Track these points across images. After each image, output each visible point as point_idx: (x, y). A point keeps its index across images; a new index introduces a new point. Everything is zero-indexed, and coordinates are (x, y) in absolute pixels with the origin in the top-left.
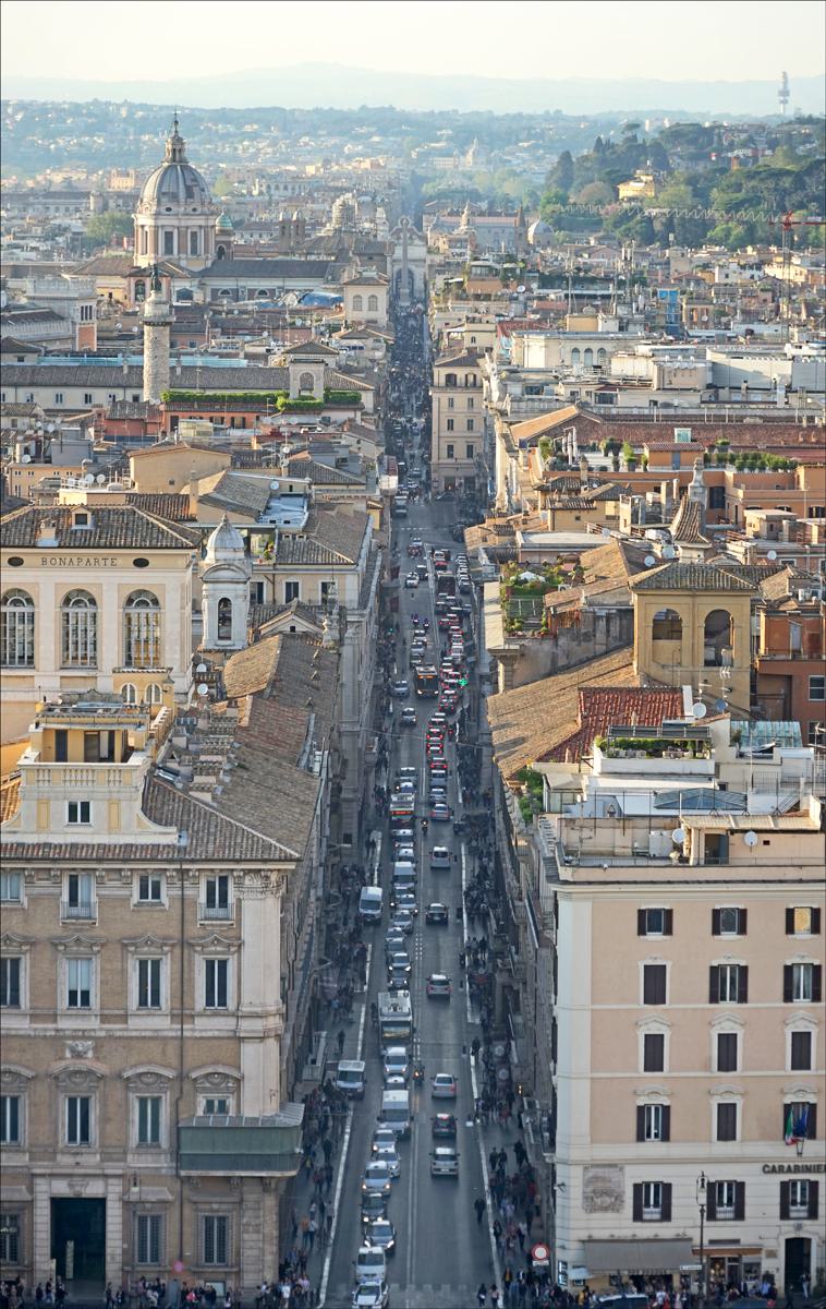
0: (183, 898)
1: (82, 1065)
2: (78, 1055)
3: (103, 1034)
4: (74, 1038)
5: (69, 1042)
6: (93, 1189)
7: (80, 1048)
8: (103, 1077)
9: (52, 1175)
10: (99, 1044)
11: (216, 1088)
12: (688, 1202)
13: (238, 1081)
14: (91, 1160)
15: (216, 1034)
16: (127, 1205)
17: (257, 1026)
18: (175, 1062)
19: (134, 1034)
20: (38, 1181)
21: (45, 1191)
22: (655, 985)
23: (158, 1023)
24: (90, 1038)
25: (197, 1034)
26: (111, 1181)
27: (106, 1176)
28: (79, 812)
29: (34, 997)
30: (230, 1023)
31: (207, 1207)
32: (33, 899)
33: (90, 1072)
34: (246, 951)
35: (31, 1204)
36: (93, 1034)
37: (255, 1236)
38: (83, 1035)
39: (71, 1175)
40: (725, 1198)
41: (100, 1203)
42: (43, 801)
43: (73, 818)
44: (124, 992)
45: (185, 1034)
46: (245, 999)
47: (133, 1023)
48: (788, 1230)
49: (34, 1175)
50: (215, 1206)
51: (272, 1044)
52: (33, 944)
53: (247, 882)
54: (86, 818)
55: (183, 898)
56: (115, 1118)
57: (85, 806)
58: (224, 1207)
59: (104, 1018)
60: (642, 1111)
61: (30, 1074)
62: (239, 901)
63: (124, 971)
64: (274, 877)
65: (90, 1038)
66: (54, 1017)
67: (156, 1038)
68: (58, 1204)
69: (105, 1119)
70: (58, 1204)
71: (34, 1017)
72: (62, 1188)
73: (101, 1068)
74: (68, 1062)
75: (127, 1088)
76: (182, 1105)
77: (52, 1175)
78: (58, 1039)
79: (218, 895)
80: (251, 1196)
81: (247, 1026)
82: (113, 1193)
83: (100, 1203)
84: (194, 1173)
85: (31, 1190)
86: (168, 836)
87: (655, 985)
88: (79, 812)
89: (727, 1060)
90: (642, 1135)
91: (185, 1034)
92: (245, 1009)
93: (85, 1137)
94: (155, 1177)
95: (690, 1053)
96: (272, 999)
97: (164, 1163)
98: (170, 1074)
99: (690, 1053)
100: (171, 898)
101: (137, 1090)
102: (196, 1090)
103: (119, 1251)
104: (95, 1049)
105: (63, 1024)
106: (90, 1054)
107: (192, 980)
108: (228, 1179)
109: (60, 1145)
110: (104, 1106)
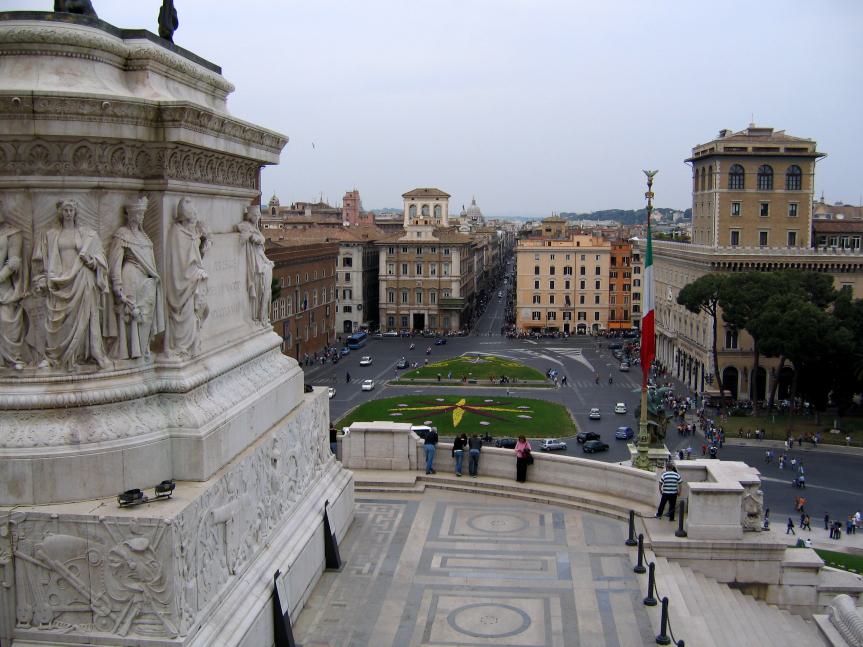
6: (422, 312)
10: (423, 282)
12: (544, 315)
16: (429, 315)
21: (412, 313)
22: (537, 270)
23: (434, 278)
28: (419, 234)
40: (551, 315)
41: (423, 315)
42: (412, 232)
48: (565, 322)
51: (458, 283)
60: (534, 297)
68: (415, 315)
70: (415, 315)
72: (416, 312)
79: (447, 252)
83: (423, 315)
87: (537, 270)
88: (419, 234)
89: (552, 286)
90: (534, 301)
95: (544, 286)
96: (458, 274)
97: (436, 307)
99: (544, 286)
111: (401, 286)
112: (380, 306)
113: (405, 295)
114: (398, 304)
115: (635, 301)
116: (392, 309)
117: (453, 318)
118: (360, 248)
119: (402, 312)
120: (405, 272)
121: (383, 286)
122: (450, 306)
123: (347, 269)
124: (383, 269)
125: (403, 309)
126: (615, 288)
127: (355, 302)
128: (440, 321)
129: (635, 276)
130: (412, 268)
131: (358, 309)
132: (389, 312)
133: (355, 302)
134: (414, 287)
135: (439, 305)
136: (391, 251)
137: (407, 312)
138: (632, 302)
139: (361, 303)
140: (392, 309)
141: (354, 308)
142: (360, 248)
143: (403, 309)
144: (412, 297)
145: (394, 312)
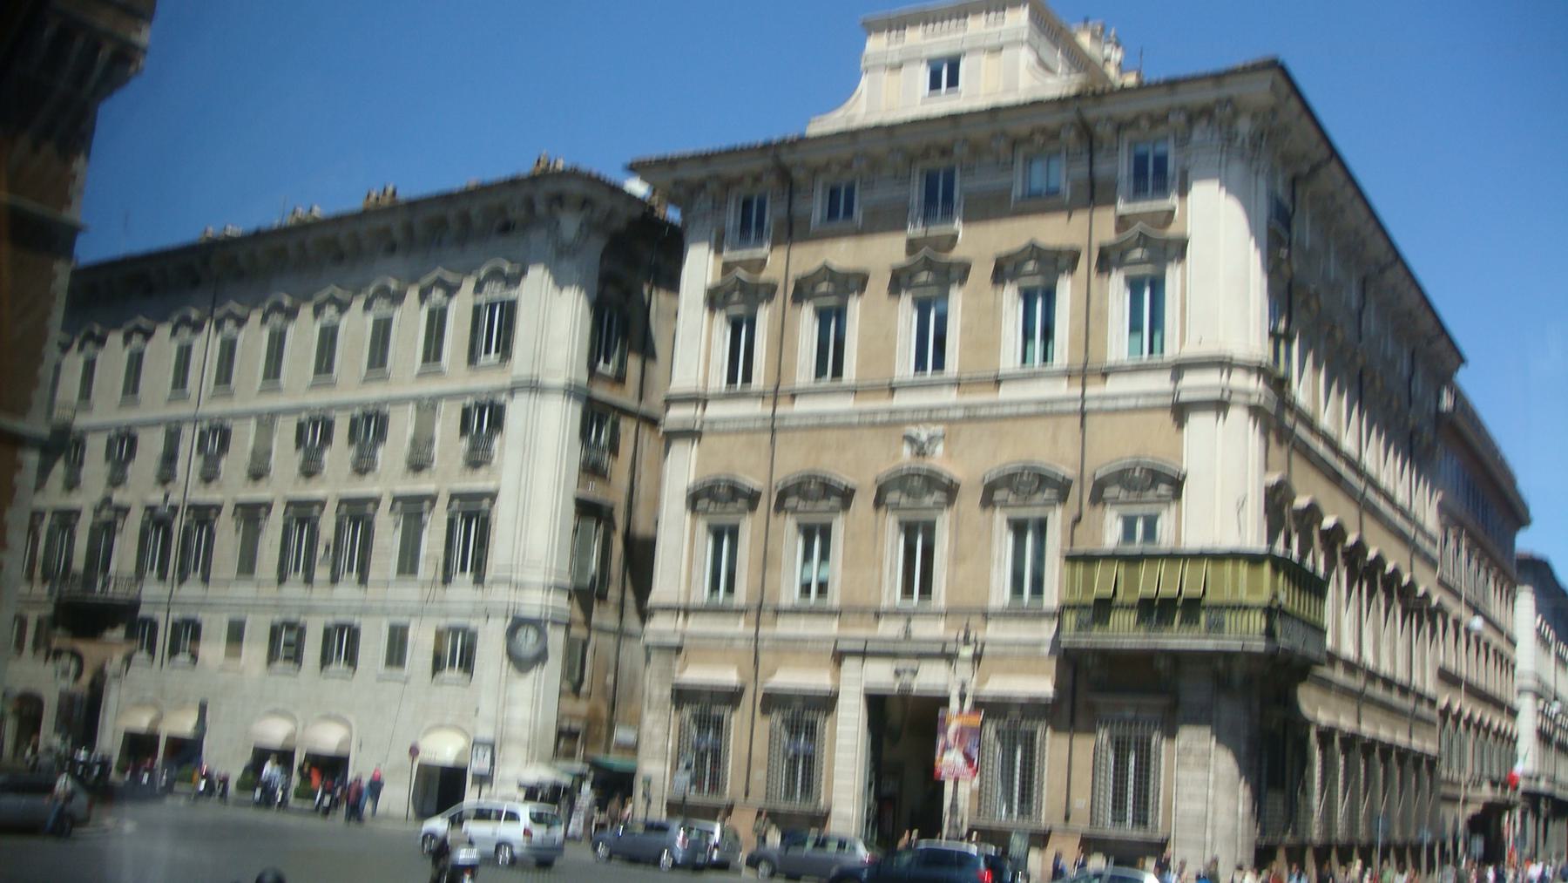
4: (916, 423)
6: (931, 678)
18: (1073, 454)
19: (1007, 410)
25: (1109, 404)
29: (863, 364)
36: (943, 414)
37: (1199, 775)
38: (930, 416)
45: (1088, 405)
47: (1007, 393)
56: (978, 556)
63: (995, 312)
64: (1244, 126)
67: (1045, 412)
69: (957, 558)
72: (881, 675)
77: (864, 655)
78: (893, 422)
81: (1197, 384)
85: (836, 677)
92: (1191, 350)
93: (926, 589)
105: (902, 400)
107: (1103, 315)
113: (816, 535)
122: (1155, 610)
125: (793, 648)
127: (499, 595)
128: (1070, 767)
130: (882, 327)
132: (696, 674)
133: (499, 595)
139: (535, 602)
140: (717, 648)
142: (570, 225)
143: (793, 648)
144: (868, 553)
145: (728, 676)
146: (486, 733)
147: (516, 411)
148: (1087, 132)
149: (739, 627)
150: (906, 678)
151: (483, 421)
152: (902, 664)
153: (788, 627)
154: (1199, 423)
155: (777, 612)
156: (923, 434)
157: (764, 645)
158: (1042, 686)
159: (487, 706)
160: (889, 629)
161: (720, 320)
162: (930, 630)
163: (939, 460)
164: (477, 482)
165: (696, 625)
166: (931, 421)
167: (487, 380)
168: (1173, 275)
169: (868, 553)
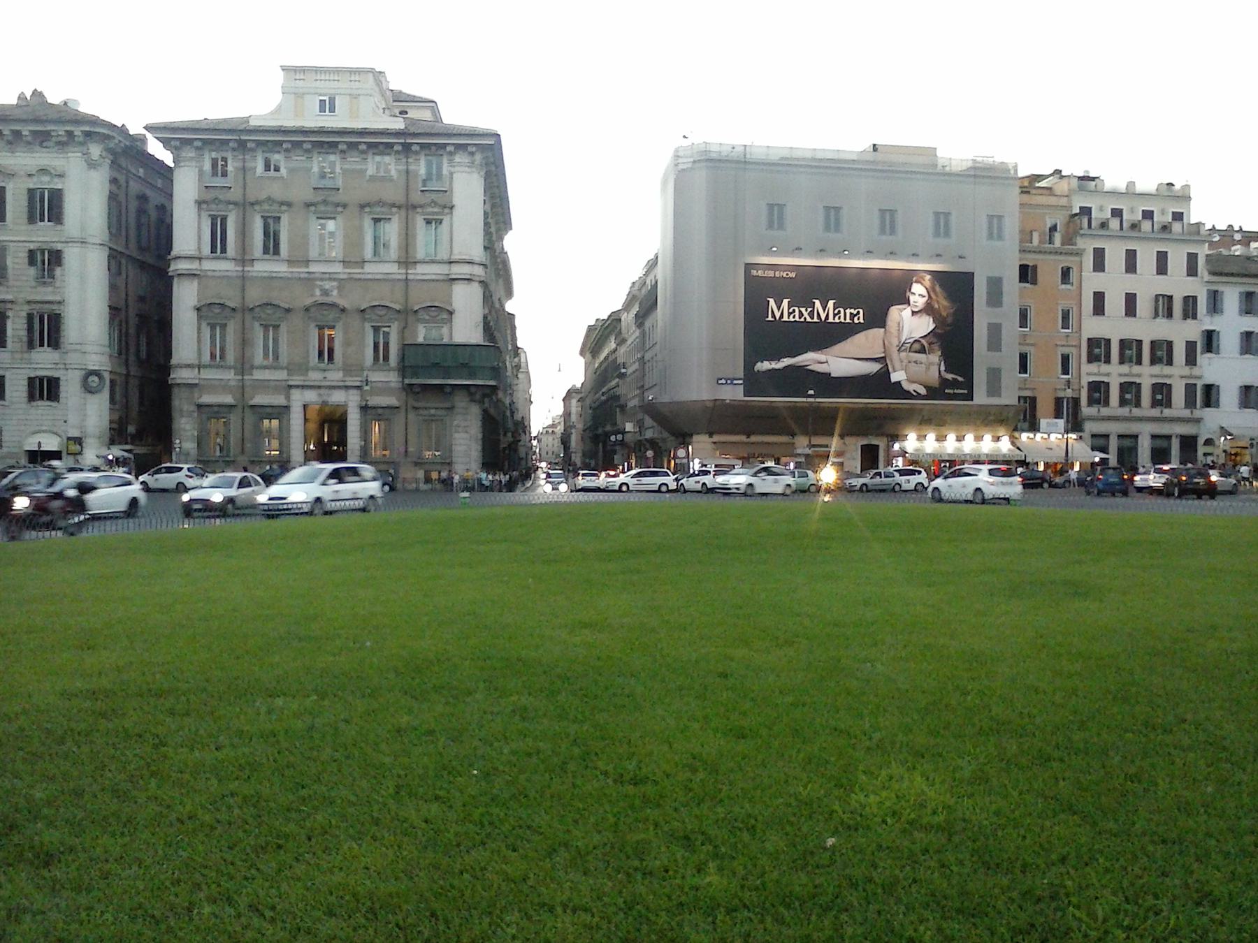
0: (407, 172)
1: (329, 300)
2: (326, 293)
3: (345, 276)
4: (322, 280)
5: (318, 283)
6: (337, 397)
7: (327, 287)
8: (343, 310)
9: (303, 387)
11: (434, 320)
13: (451, 313)
14: (335, 376)
15: (434, 277)
16: (364, 409)
17: (464, 270)
19: (370, 277)
20: (293, 391)
24: (335, 280)
26: (352, 392)
27: (347, 387)
28: (328, 106)
30: (442, 269)
31: (425, 412)
32: (291, 171)
33: (333, 305)
34: (455, 212)
35: (287, 408)
37: (465, 435)
38: (331, 277)
39: (319, 387)
43: (322, 110)
44: (360, 244)
46: (456, 251)
47: (369, 268)
49: (291, 387)
50: (433, 411)
52: (289, 205)
53: (457, 158)
54: (332, 110)
55: (407, 172)
57: (332, 101)
58: (439, 412)
59: (345, 263)
61: (287, 306)
62: (451, 174)
65: (335, 280)
66: (307, 262)
67: (386, 280)
71: (290, 262)
73: (342, 302)
74: (318, 296)
75: (365, 320)
76: (403, 325)
77: (303, 387)
78: (309, 280)
80: (461, 401)
81: (458, 270)
82: (351, 402)
84: (414, 381)
85: (288, 398)
86: (398, 124)
91: (410, 277)
92: (455, 257)
94: (384, 390)
97: (393, 378)
98: (397, 307)
100: (399, 171)
101: (370, 320)
102: (418, 320)
103: (358, 447)
104: (338, 288)
106: (335, 293)
108: (441, 387)
109: (311, 364)
110: (346, 332)
111: (255, 296)
112: (180, 376)
114: (243, 366)
115: (1093, 368)
116: (224, 387)
117: (458, 421)
118: (95, 150)
119: (259, 400)
120: (272, 245)
121: (185, 298)
123: (43, 234)
124: (188, 232)
125: (263, 386)
126: (1031, 315)
129: (1091, 282)
131: (88, 390)
132: (206, 399)
134: (309, 301)
135: (403, 370)
136: (219, 169)
137: (279, 400)
138: (1087, 368)
141: (70, 388)
142: (95, 150)
145: (229, 399)
146: (75, 433)
147: (71, 256)
148: (407, 147)
149: (230, 376)
150: (325, 398)
151: (48, 262)
152: (322, 391)
153: (258, 375)
154: (459, 290)
155: (252, 367)
156: (327, 285)
157: (247, 383)
158: (392, 401)
159: (73, 419)
160: (315, 376)
161: (204, 215)
162: (335, 376)
163: (334, 297)
164: (45, 294)
165: (207, 374)
166: (330, 279)
167: (43, 234)
168: (446, 219)
169: (298, 341)
